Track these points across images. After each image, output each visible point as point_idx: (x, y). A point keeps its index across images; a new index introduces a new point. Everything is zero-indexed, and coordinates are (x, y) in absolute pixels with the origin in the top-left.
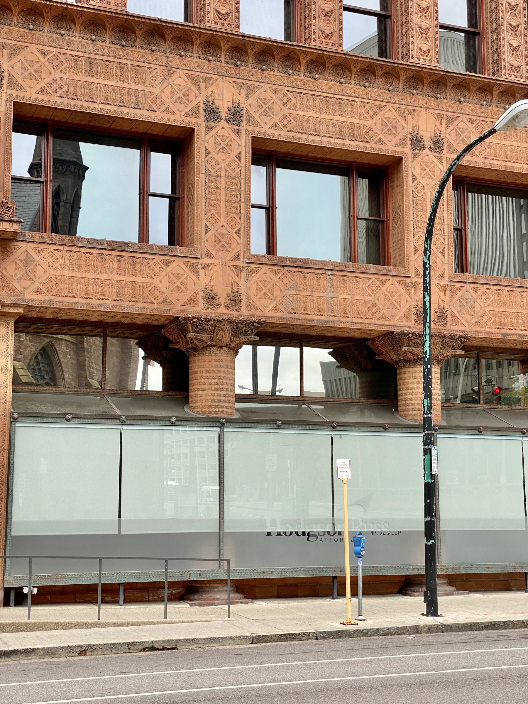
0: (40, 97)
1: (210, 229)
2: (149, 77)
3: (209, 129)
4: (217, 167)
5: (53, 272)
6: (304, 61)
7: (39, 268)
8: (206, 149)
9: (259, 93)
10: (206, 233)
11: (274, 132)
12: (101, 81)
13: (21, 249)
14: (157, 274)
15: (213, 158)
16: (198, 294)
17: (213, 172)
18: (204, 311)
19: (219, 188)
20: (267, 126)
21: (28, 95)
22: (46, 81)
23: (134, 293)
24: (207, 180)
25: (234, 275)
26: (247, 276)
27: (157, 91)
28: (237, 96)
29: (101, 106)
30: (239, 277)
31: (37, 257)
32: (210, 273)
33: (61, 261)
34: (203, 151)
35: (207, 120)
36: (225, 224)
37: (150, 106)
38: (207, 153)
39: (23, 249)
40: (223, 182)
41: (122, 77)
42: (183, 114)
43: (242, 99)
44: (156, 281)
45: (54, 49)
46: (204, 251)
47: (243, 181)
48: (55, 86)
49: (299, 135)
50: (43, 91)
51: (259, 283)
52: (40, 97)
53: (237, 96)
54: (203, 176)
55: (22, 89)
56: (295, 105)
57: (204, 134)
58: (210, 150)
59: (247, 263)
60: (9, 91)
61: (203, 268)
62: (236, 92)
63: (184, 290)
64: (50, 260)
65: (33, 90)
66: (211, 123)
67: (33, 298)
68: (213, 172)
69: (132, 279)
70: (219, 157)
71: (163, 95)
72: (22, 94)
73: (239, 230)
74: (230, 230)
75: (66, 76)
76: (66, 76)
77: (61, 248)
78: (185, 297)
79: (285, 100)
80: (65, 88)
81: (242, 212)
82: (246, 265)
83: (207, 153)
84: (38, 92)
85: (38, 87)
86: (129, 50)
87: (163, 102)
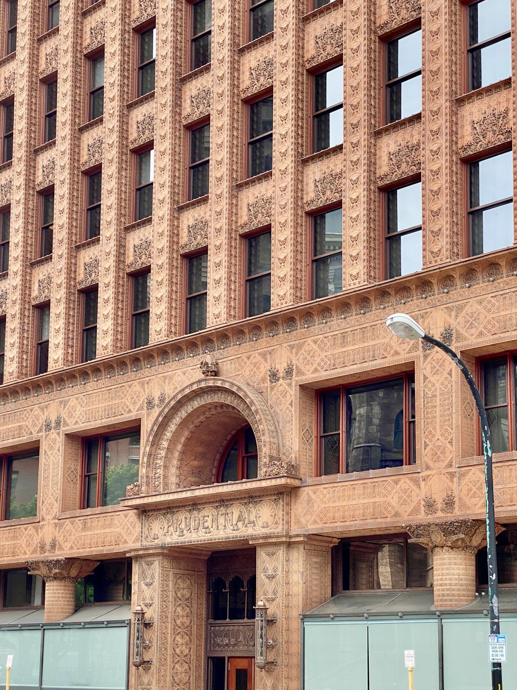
0: (314, 375)
1: (428, 445)
2: (382, 332)
3: (426, 357)
4: (433, 389)
5: (323, 506)
6: (503, 263)
7: (316, 505)
8: (424, 376)
9: (468, 309)
10: (425, 449)
11: (479, 340)
12: (351, 348)
13: (305, 493)
14: (390, 493)
15: (430, 382)
16: (420, 504)
17: (430, 394)
18: (425, 517)
19: (435, 407)
20: (474, 337)
21: (307, 377)
22: (317, 362)
23: (374, 512)
24: (425, 402)
25: (448, 481)
26: (459, 479)
27: (387, 340)
28: (448, 319)
29: (351, 367)
30: (452, 481)
31: (313, 497)
32: (429, 483)
33: (328, 496)
34: (422, 377)
35: (425, 350)
36: (440, 437)
37: (383, 354)
38: (425, 378)
39: (305, 493)
40: (438, 400)
41: (363, 339)
42: (406, 352)
43: (451, 321)
44: (389, 499)
45: (321, 336)
46: (424, 465)
47: (454, 394)
48: (322, 363)
49: (502, 335)
50: (316, 370)
51: (470, 484)
52: (314, 375)
53: (448, 319)
54: (422, 400)
55: (303, 374)
56: (498, 309)
57: (422, 363)
58: (427, 375)
59: (458, 467)
60: (297, 379)
61: (424, 480)
62: (447, 316)
63: (410, 502)
64: (322, 497)
65: (310, 372)
66: (428, 352)
67: (313, 528)
68: (430, 394)
69: (373, 500)
70: (433, 379)
71: (392, 342)
72: (303, 378)
73: (452, 439)
74: (444, 441)
75: (329, 353)
76: (329, 353)
77: (327, 486)
78: (409, 509)
79: (489, 306)
80: (329, 362)
81: (454, 422)
82: (458, 470)
83: (425, 378)
84: (313, 372)
85: (312, 369)
86: (367, 315)
87: (391, 348)
